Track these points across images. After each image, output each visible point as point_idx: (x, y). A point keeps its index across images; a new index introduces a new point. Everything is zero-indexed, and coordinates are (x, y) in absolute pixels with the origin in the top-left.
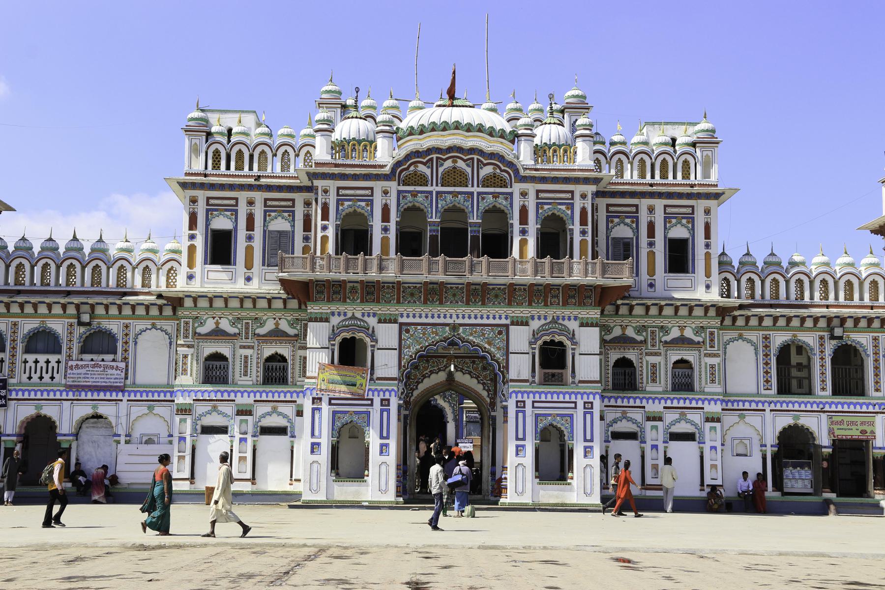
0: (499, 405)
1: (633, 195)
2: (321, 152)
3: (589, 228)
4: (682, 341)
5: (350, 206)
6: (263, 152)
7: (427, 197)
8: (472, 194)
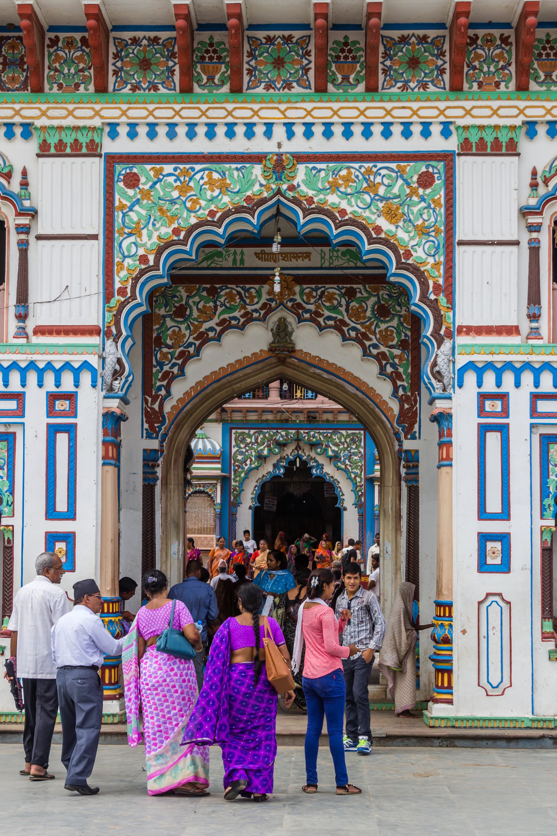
0: (425, 412)
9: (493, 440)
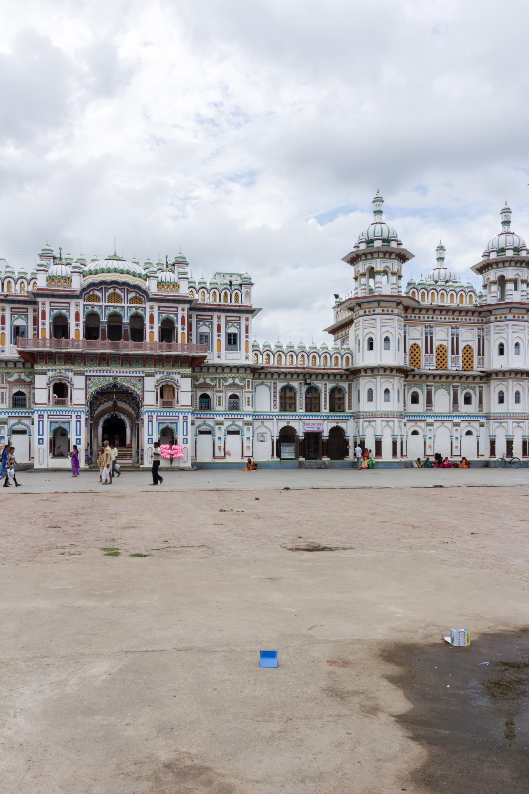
1: (210, 310)
2: (42, 282)
3: (186, 326)
4: (234, 386)
5: (57, 313)
6: (9, 282)
7: (100, 308)
8: (124, 307)
9: (150, 423)
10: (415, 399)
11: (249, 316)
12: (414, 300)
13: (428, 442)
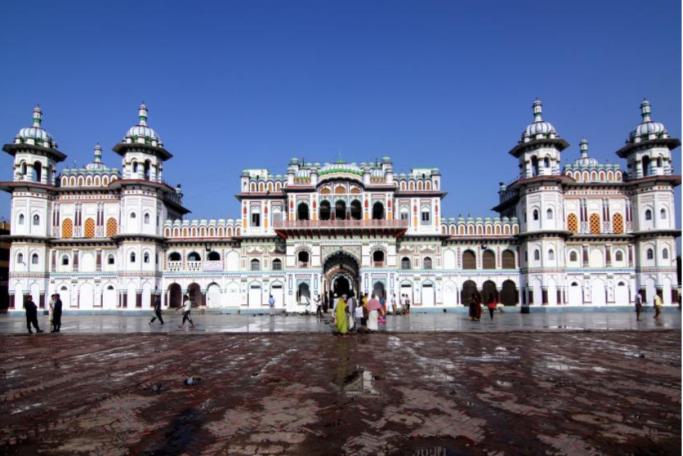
10: (573, 257)
11: (438, 199)
12: (569, 176)
13: (586, 292)
